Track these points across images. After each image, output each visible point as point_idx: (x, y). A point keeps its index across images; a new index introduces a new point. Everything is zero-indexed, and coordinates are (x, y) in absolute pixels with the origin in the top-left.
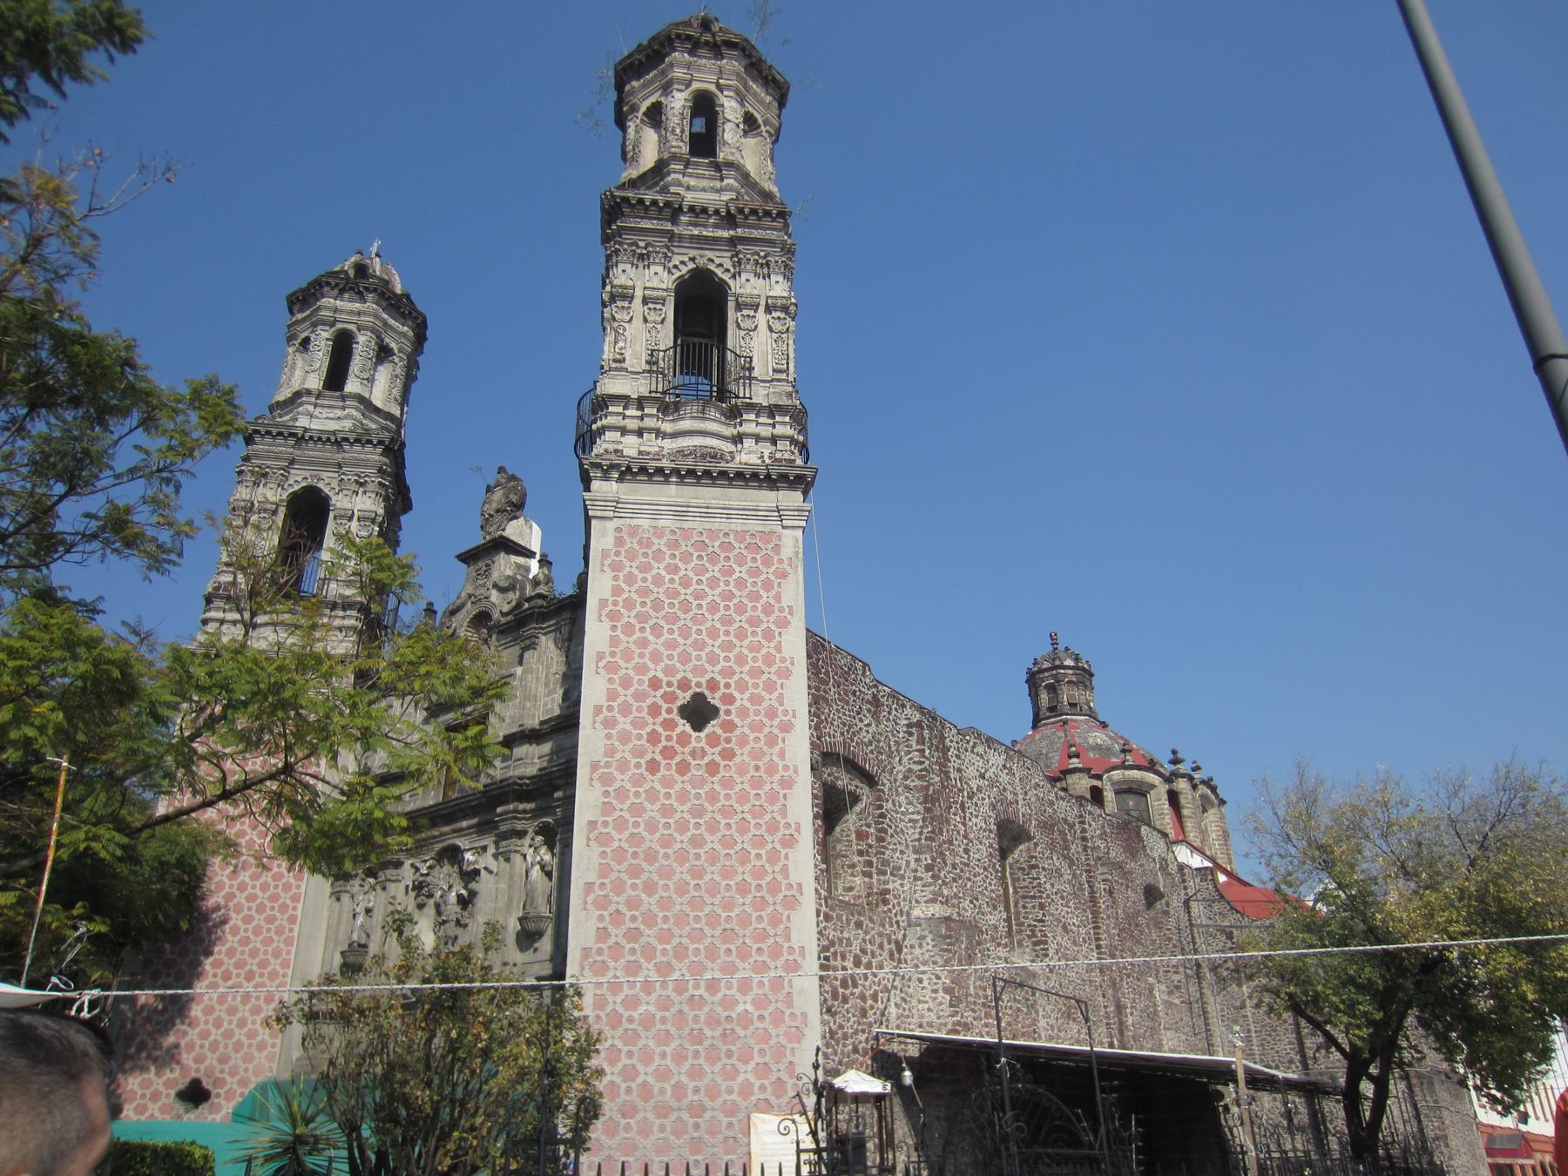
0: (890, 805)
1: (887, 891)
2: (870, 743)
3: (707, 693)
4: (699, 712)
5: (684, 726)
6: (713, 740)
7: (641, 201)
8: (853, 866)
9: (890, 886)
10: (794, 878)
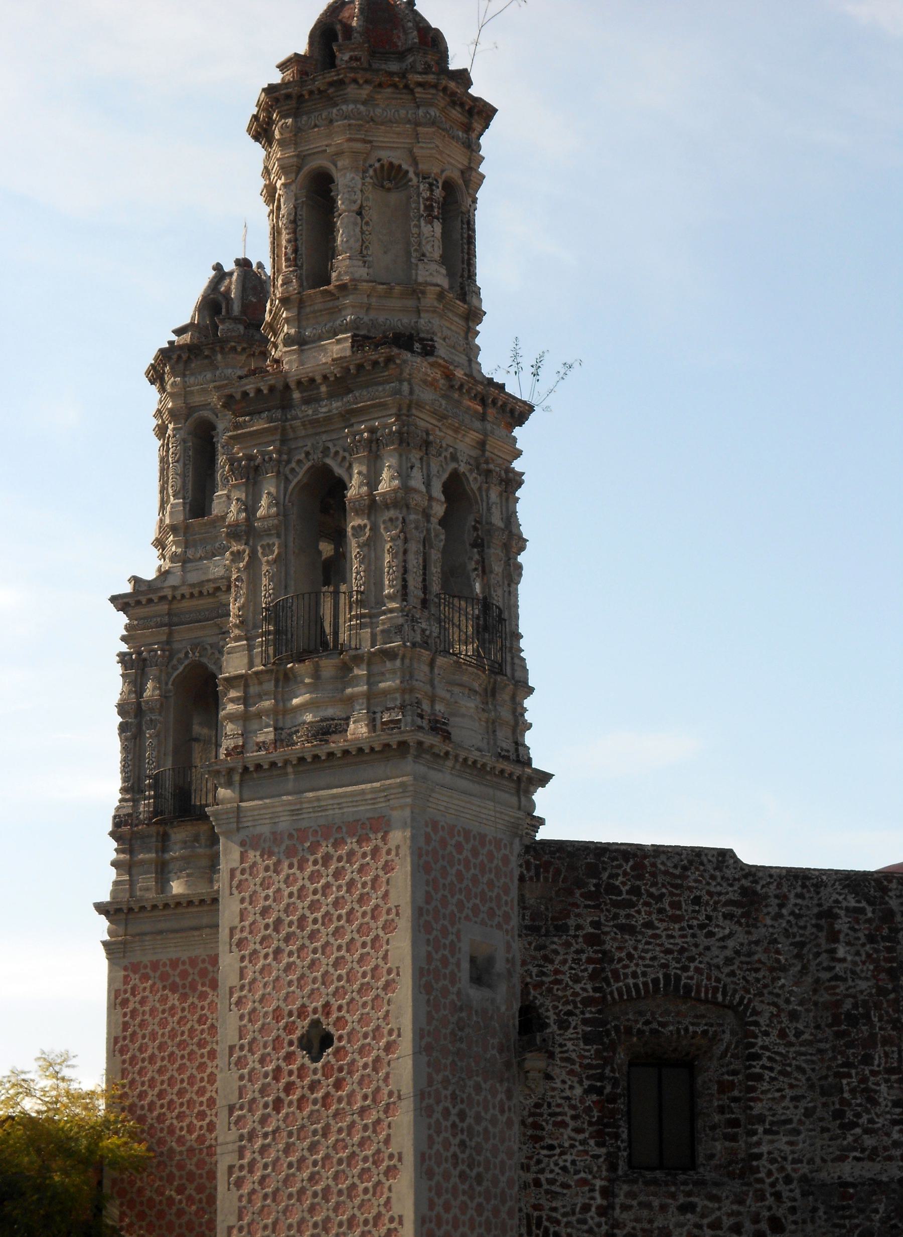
0: (774, 1037)
1: (759, 1156)
2: (729, 961)
3: (322, 1019)
4: (318, 1041)
5: (302, 1058)
6: (327, 1070)
7: (245, 394)
8: (713, 1128)
9: (764, 1149)
10: (396, 1211)
